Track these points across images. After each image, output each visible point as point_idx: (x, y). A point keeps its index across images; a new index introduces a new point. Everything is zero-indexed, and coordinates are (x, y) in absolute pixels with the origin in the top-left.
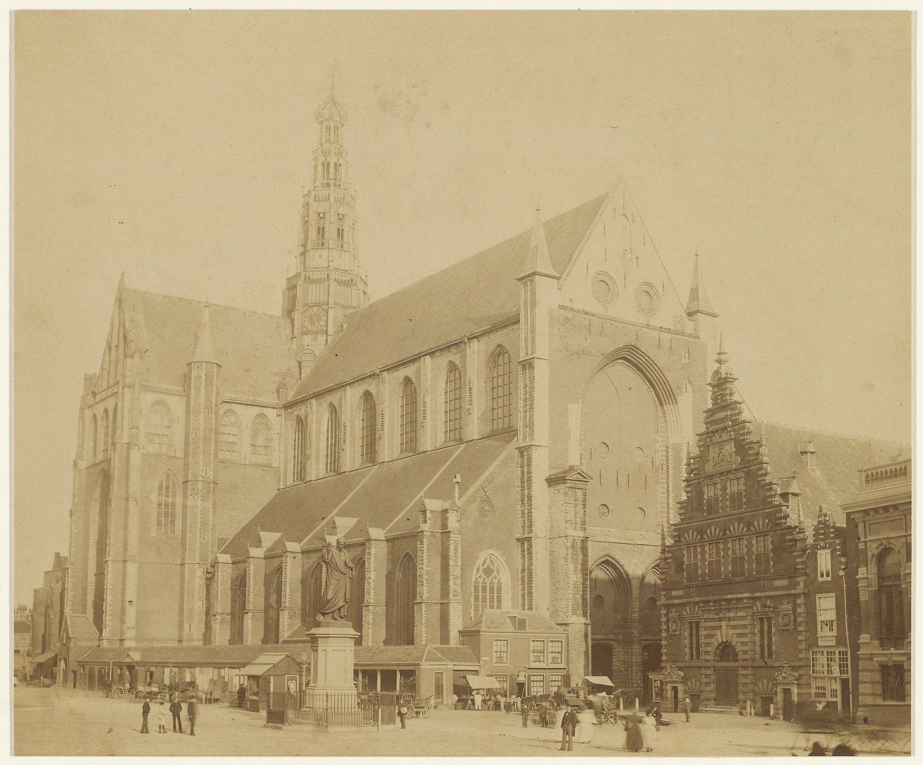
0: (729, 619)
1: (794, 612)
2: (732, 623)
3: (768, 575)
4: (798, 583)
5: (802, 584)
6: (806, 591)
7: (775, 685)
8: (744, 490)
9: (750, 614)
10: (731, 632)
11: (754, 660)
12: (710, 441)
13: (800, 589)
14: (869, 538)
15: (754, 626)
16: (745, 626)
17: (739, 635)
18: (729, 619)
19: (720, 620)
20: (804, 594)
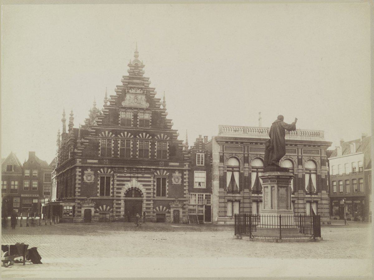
0: (138, 177)
1: (183, 178)
2: (139, 179)
3: (166, 160)
4: (185, 165)
5: (187, 166)
6: (190, 169)
7: (170, 208)
8: (151, 119)
9: (153, 176)
10: (139, 183)
11: (154, 197)
12: (127, 91)
13: (186, 167)
14: (251, 153)
15: (154, 182)
16: (150, 181)
17: (144, 185)
18: (138, 177)
19: (130, 177)
20: (189, 170)
